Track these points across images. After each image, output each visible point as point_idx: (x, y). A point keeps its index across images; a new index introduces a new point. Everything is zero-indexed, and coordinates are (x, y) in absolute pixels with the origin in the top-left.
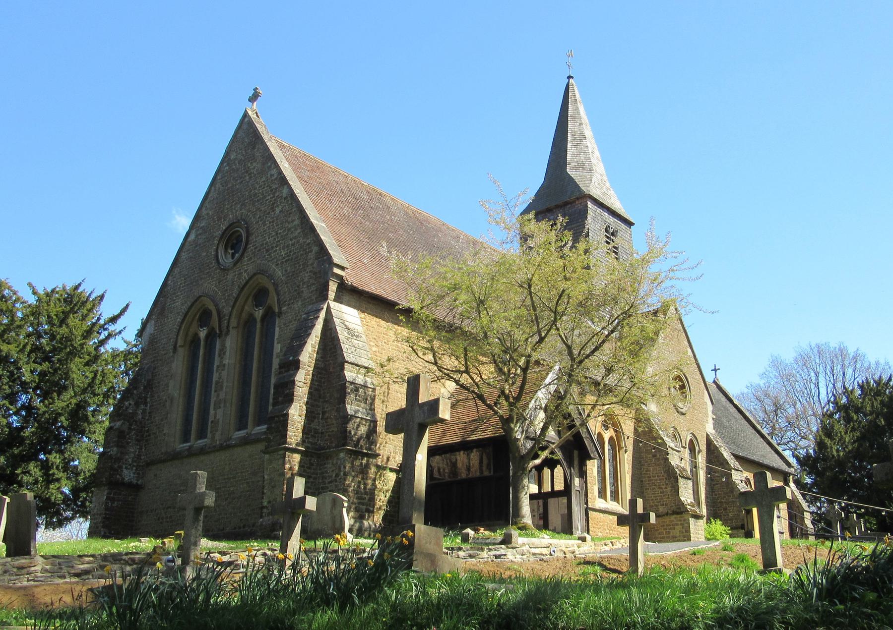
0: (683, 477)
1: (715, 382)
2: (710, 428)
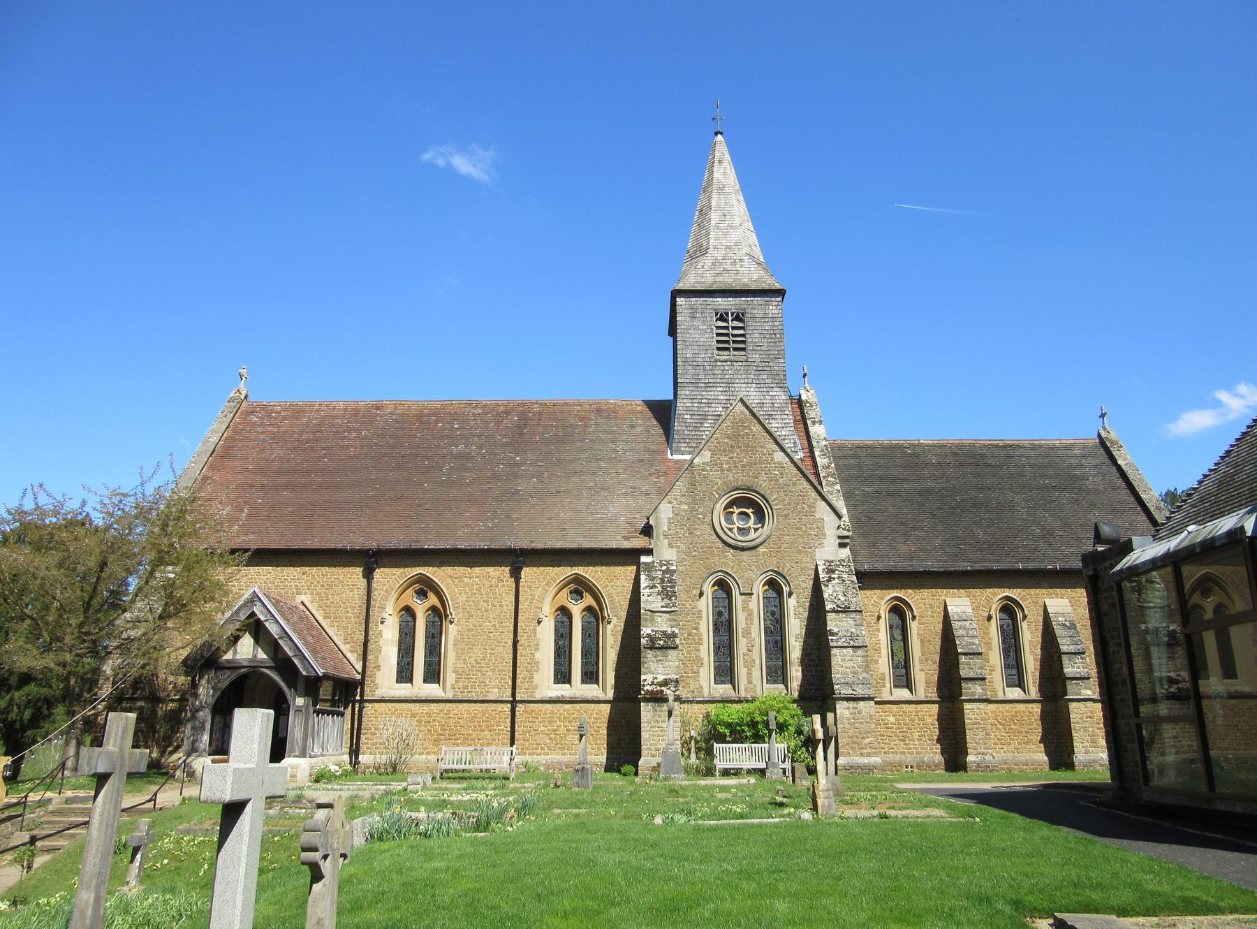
0: (651, 648)
1: (1099, 436)
2: (829, 551)
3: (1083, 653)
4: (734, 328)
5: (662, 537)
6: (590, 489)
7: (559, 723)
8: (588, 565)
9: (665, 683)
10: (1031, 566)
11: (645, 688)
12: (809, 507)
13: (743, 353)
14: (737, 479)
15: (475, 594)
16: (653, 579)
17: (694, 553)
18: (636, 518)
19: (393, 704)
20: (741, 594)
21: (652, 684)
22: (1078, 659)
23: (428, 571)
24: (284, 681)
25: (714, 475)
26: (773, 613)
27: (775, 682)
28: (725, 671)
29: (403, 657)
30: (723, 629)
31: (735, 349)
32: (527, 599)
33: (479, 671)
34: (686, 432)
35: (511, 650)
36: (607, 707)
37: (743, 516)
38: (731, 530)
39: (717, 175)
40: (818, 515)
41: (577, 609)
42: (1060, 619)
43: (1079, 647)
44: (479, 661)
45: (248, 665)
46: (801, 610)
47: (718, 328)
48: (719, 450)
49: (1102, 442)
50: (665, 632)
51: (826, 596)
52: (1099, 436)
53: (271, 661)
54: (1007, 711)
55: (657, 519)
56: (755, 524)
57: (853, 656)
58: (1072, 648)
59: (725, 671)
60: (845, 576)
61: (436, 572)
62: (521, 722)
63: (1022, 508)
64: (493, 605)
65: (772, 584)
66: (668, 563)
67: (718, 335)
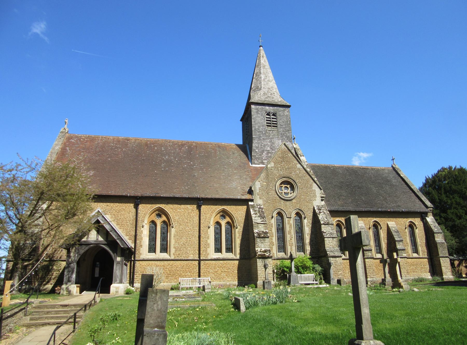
0: (259, 238)
1: (392, 166)
2: (318, 202)
3: (402, 241)
4: (273, 118)
5: (257, 195)
6: (223, 176)
7: (218, 269)
8: (228, 205)
9: (265, 251)
10: (383, 210)
11: (258, 253)
12: (310, 185)
13: (276, 128)
14: (284, 174)
15: (182, 216)
16: (255, 211)
17: (269, 202)
18: (244, 188)
19: (148, 262)
20: (287, 218)
21: (260, 252)
22: (401, 243)
23: (163, 206)
24: (111, 250)
25: (275, 172)
26: (298, 225)
27: (300, 251)
28: (282, 247)
29: (151, 242)
30: (280, 232)
31: (273, 126)
32: (204, 218)
33: (185, 247)
34: (257, 156)
35: (198, 239)
36: (237, 262)
37: (286, 188)
38: (282, 193)
39: (262, 61)
40: (313, 189)
41: (223, 223)
42: (393, 229)
43: (401, 239)
44: (185, 243)
45: (94, 243)
46: (309, 224)
47: (267, 118)
48: (277, 162)
49: (394, 169)
50: (263, 232)
51: (320, 218)
52: (392, 166)
53: (105, 241)
54: (377, 262)
55: (255, 188)
56: (290, 191)
57: (332, 241)
58: (399, 239)
59: (282, 247)
60: (325, 211)
61: (166, 206)
62: (203, 268)
63: (374, 190)
64: (190, 221)
65: (298, 214)
66: (260, 205)
67: (267, 120)
